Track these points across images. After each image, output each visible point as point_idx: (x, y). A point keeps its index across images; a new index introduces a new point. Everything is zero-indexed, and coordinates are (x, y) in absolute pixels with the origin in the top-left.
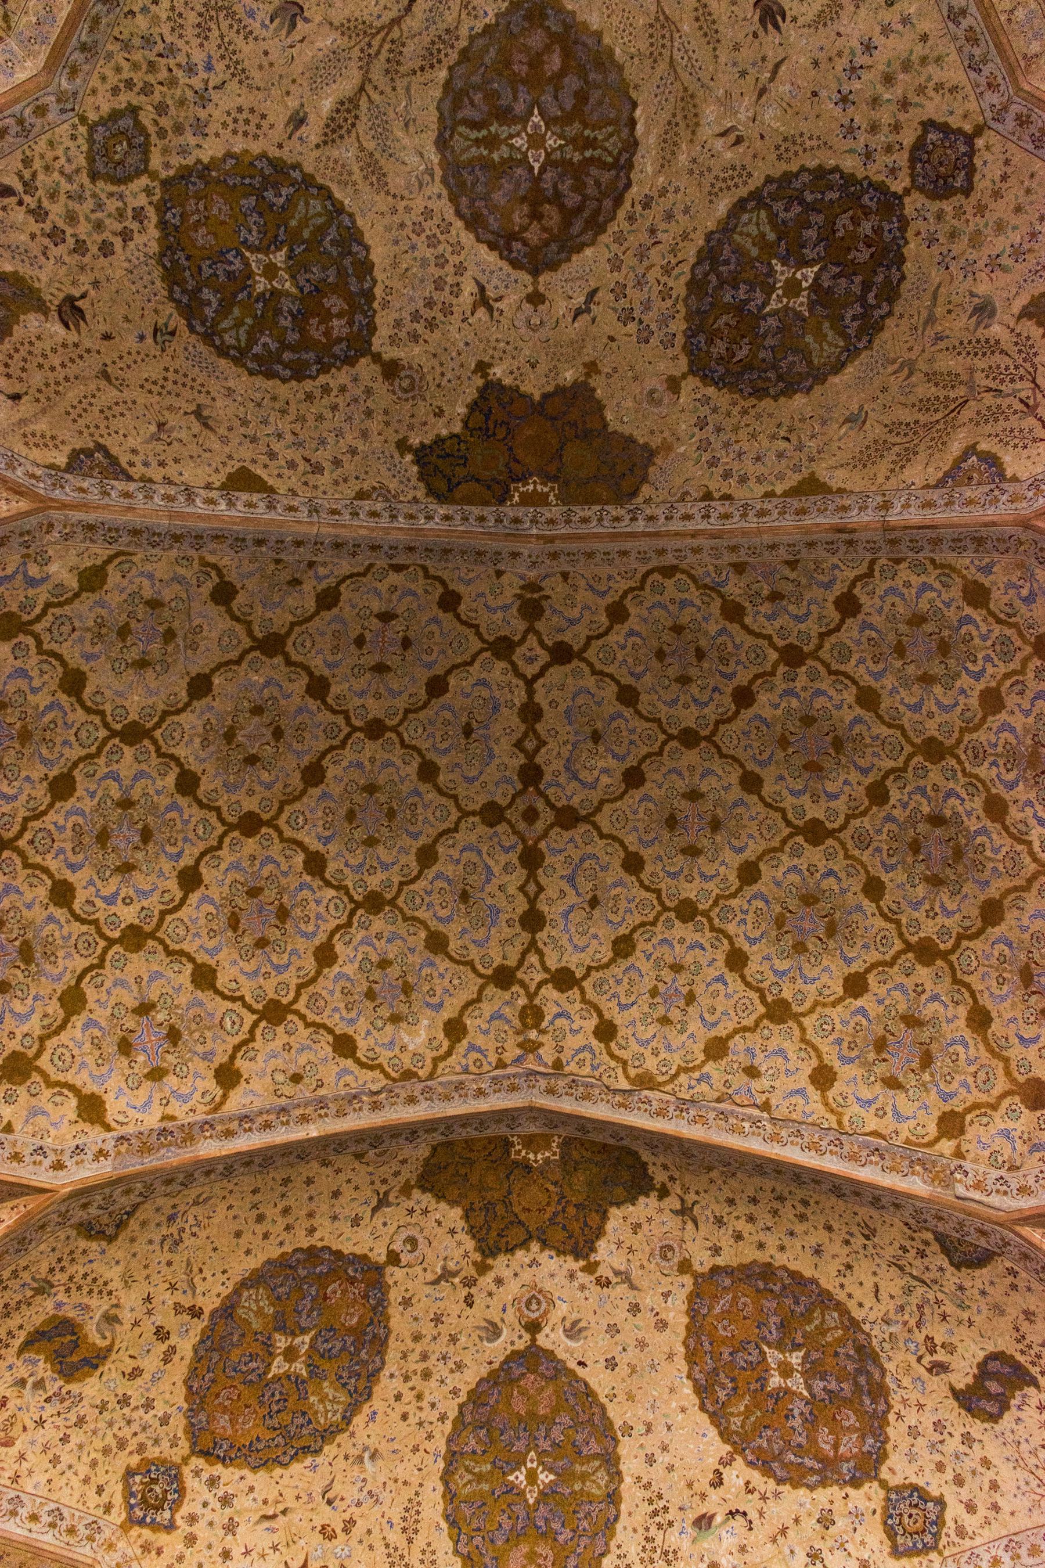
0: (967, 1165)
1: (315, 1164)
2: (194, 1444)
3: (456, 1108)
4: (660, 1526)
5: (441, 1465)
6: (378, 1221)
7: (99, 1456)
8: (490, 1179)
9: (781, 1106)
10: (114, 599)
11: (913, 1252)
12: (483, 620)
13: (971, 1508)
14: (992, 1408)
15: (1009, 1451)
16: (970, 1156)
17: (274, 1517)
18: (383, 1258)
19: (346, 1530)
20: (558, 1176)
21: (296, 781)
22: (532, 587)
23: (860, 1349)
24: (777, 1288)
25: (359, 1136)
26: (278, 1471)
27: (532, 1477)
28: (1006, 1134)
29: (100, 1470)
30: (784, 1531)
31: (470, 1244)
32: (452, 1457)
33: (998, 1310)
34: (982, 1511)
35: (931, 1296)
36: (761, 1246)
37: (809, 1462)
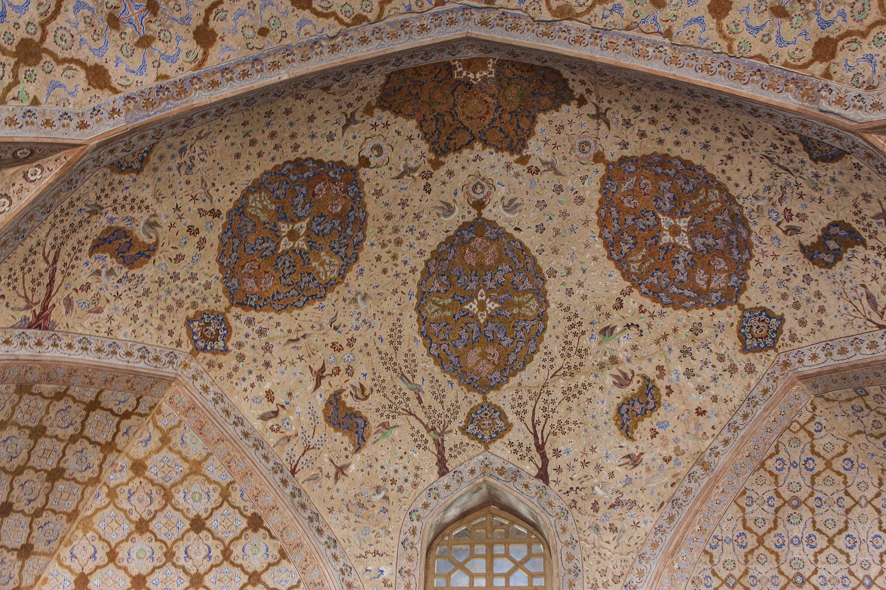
0: (833, 84)
1: (289, 98)
2: (231, 300)
3: (402, 44)
4: (575, 334)
5: (415, 301)
6: (349, 135)
7: (165, 312)
8: (438, 96)
9: (681, 33)
11: (781, 149)
13: (802, 323)
14: (828, 259)
15: (838, 288)
16: (835, 77)
17: (297, 340)
18: (356, 163)
19: (349, 345)
20: (494, 90)
23: (733, 216)
24: (672, 173)
25: (323, 74)
26: (296, 312)
27: (482, 306)
28: (870, 59)
29: (168, 320)
30: (665, 337)
31: (425, 147)
32: (422, 296)
33: (844, 192)
34: (810, 325)
35: (792, 180)
36: (661, 141)
37: (687, 292)
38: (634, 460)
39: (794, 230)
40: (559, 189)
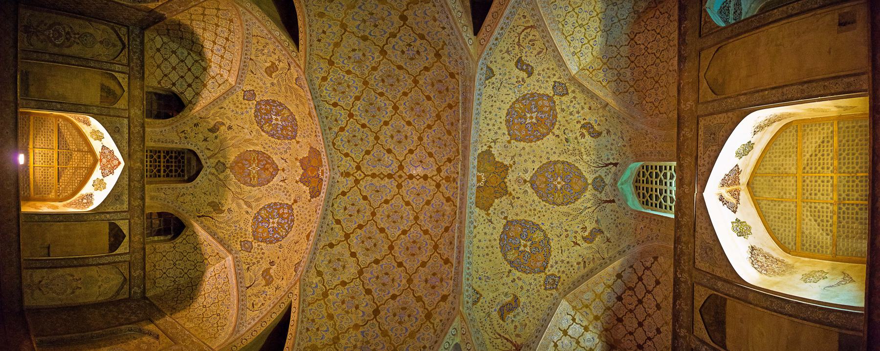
10: (326, 270)
12: (349, 186)
13: (554, 75)
21: (383, 235)
22: (342, 174)
33: (503, 65)
38: (608, 132)
39: (523, 79)
40: (520, 155)
